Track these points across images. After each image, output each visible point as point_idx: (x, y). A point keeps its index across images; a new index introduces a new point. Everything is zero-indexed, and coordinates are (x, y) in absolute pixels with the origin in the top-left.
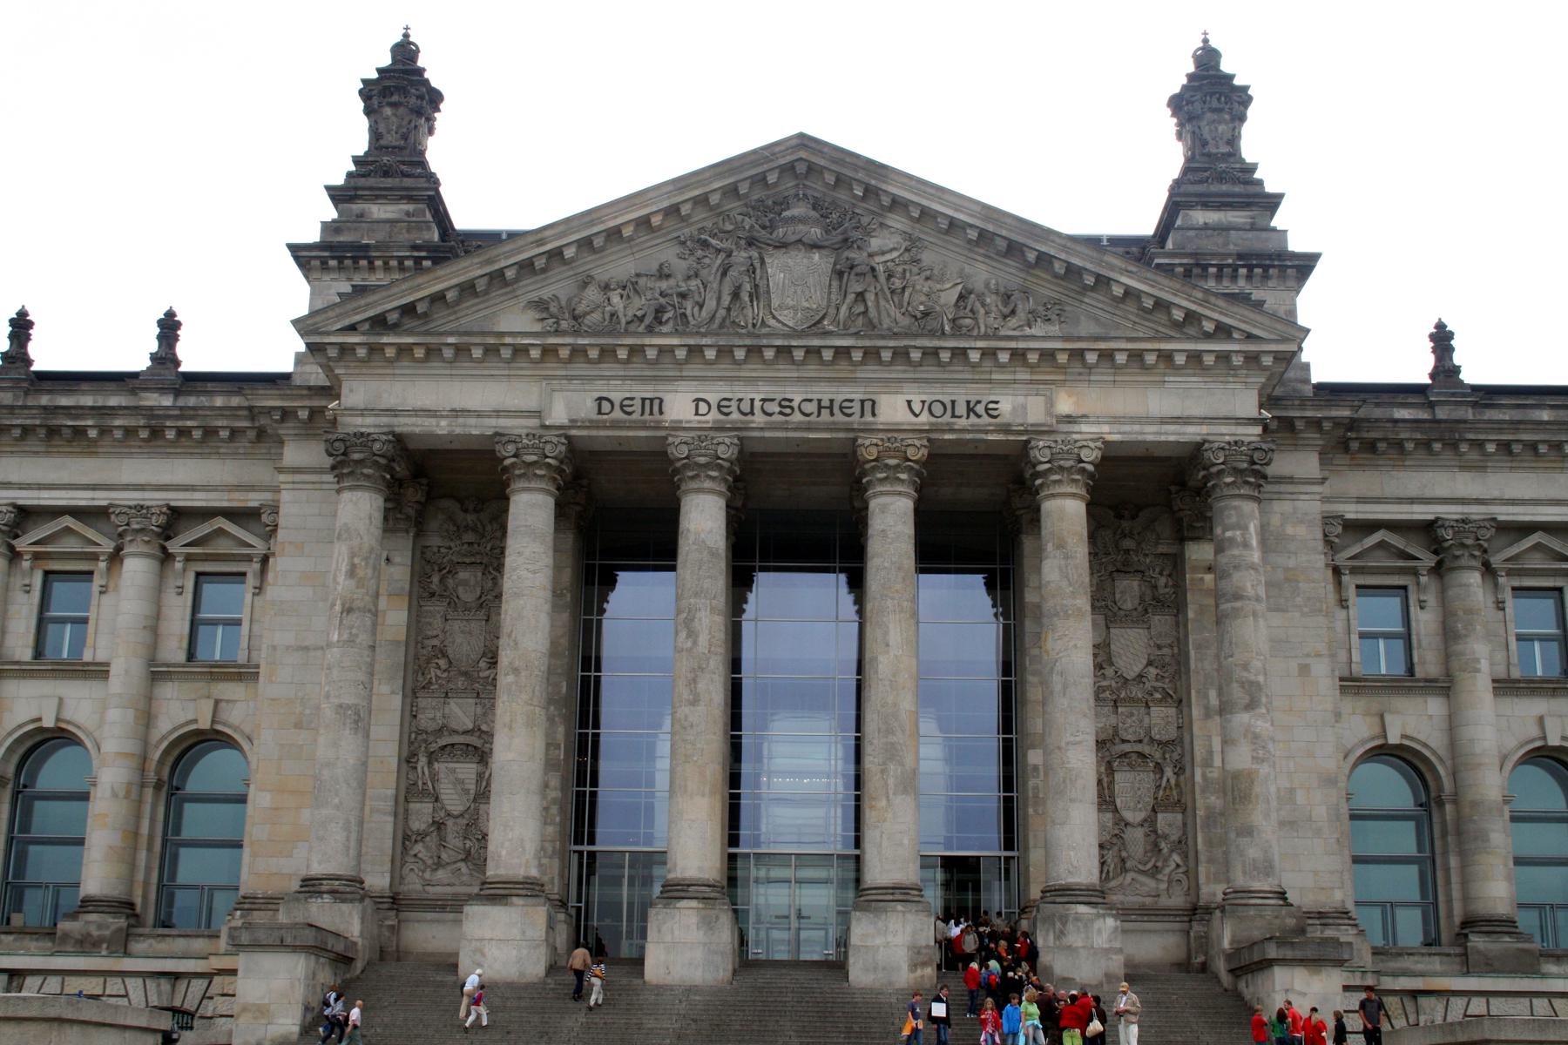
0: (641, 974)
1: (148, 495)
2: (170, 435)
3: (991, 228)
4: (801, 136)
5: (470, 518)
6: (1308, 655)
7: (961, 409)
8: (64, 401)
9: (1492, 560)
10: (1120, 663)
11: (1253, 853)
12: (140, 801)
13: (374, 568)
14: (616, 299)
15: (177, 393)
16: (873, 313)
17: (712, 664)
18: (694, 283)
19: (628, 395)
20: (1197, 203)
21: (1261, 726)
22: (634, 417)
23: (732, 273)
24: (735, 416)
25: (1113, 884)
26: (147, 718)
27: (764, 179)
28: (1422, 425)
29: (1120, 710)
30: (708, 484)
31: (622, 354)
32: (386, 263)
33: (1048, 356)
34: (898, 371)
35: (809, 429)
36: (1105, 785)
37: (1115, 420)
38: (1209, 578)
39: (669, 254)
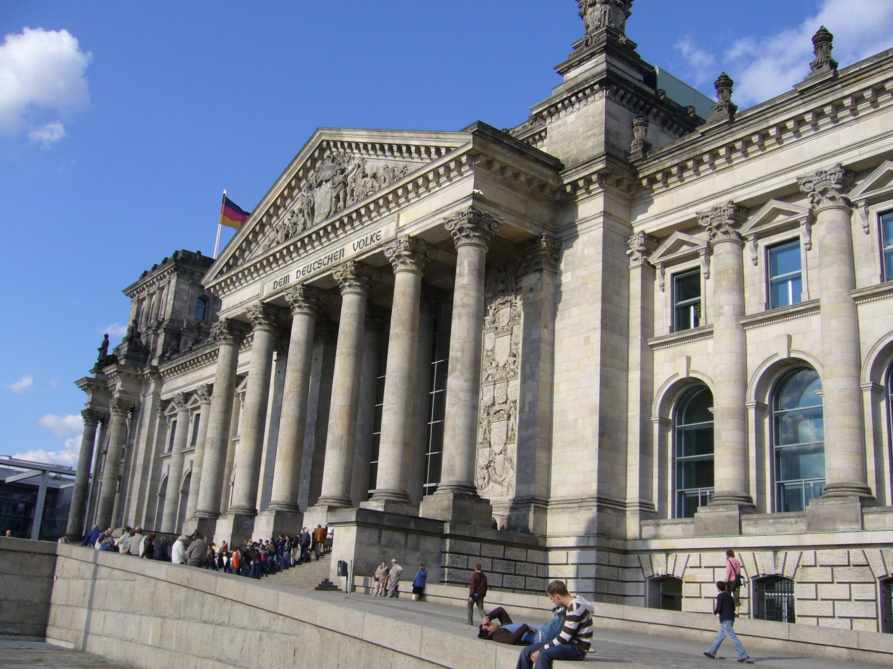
6: (589, 330)
7: (369, 242)
9: (740, 231)
10: (497, 358)
13: (225, 378)
17: (290, 396)
19: (281, 277)
20: (569, 69)
22: (282, 286)
24: (307, 274)
25: (486, 490)
28: (675, 154)
29: (497, 386)
36: (487, 431)
37: (417, 222)
38: (531, 295)
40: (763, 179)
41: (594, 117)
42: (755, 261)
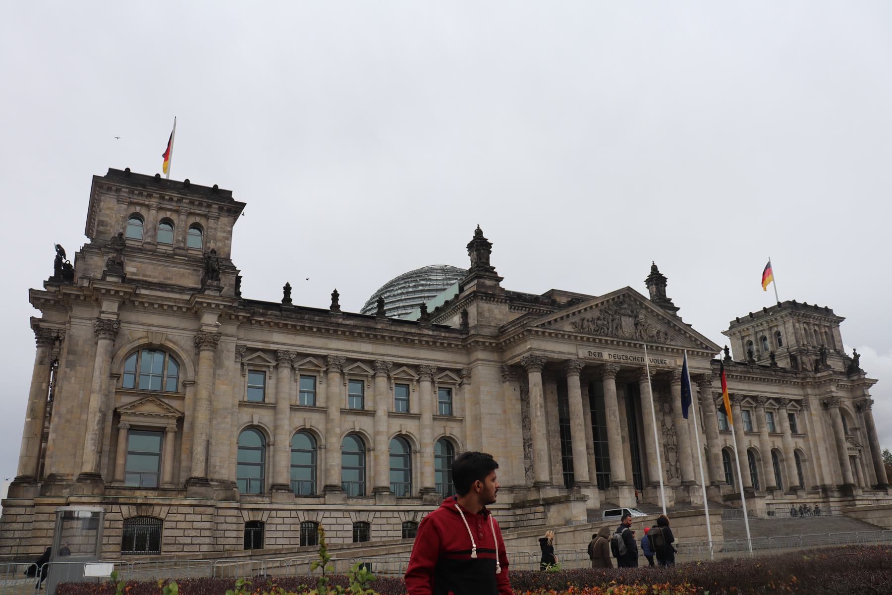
1: (429, 362)
2: (438, 344)
4: (629, 287)
7: (660, 362)
8: (399, 329)
15: (433, 330)
22: (597, 357)
23: (617, 321)
24: (617, 359)
27: (619, 297)
33: (678, 350)
35: (632, 364)
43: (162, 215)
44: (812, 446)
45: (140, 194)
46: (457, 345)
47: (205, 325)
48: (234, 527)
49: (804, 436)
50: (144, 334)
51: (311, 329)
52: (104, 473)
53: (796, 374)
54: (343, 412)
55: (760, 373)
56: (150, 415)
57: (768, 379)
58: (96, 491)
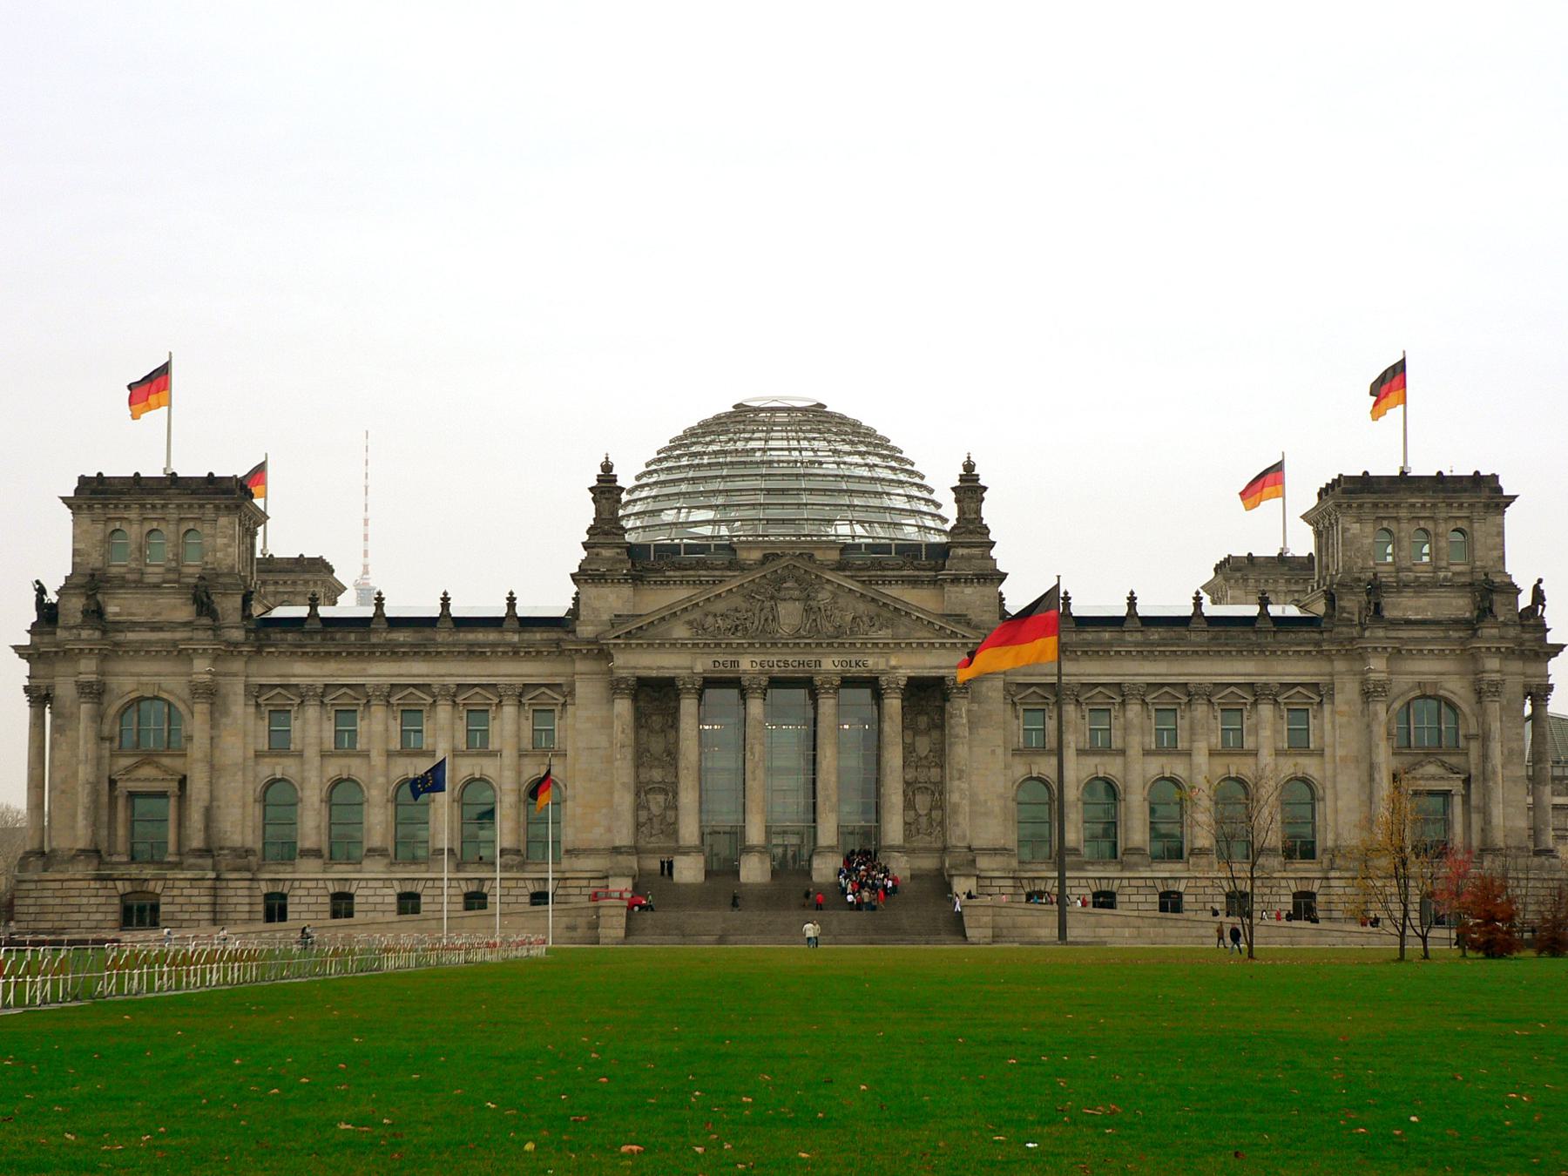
0: (739, 880)
2: (522, 654)
3: (864, 592)
5: (656, 694)
7: (853, 664)
8: (471, 637)
11: (958, 832)
12: (519, 809)
14: (719, 621)
16: (819, 626)
18: (750, 614)
21: (965, 786)
24: (767, 667)
26: (519, 773)
30: (757, 695)
31: (723, 646)
32: (612, 580)
34: (829, 650)
37: (914, 668)
39: (738, 601)
40: (1099, 675)
41: (989, 598)
42: (1083, 717)
43: (147, 527)
44: (1329, 773)
45: (116, 506)
46: (549, 653)
47: (195, 673)
48: (247, 900)
49: (1321, 753)
50: (135, 687)
51: (339, 654)
52: (103, 846)
53: (1321, 632)
54: (390, 754)
55: (1213, 639)
56: (147, 780)
57: (1219, 651)
58: (90, 868)
